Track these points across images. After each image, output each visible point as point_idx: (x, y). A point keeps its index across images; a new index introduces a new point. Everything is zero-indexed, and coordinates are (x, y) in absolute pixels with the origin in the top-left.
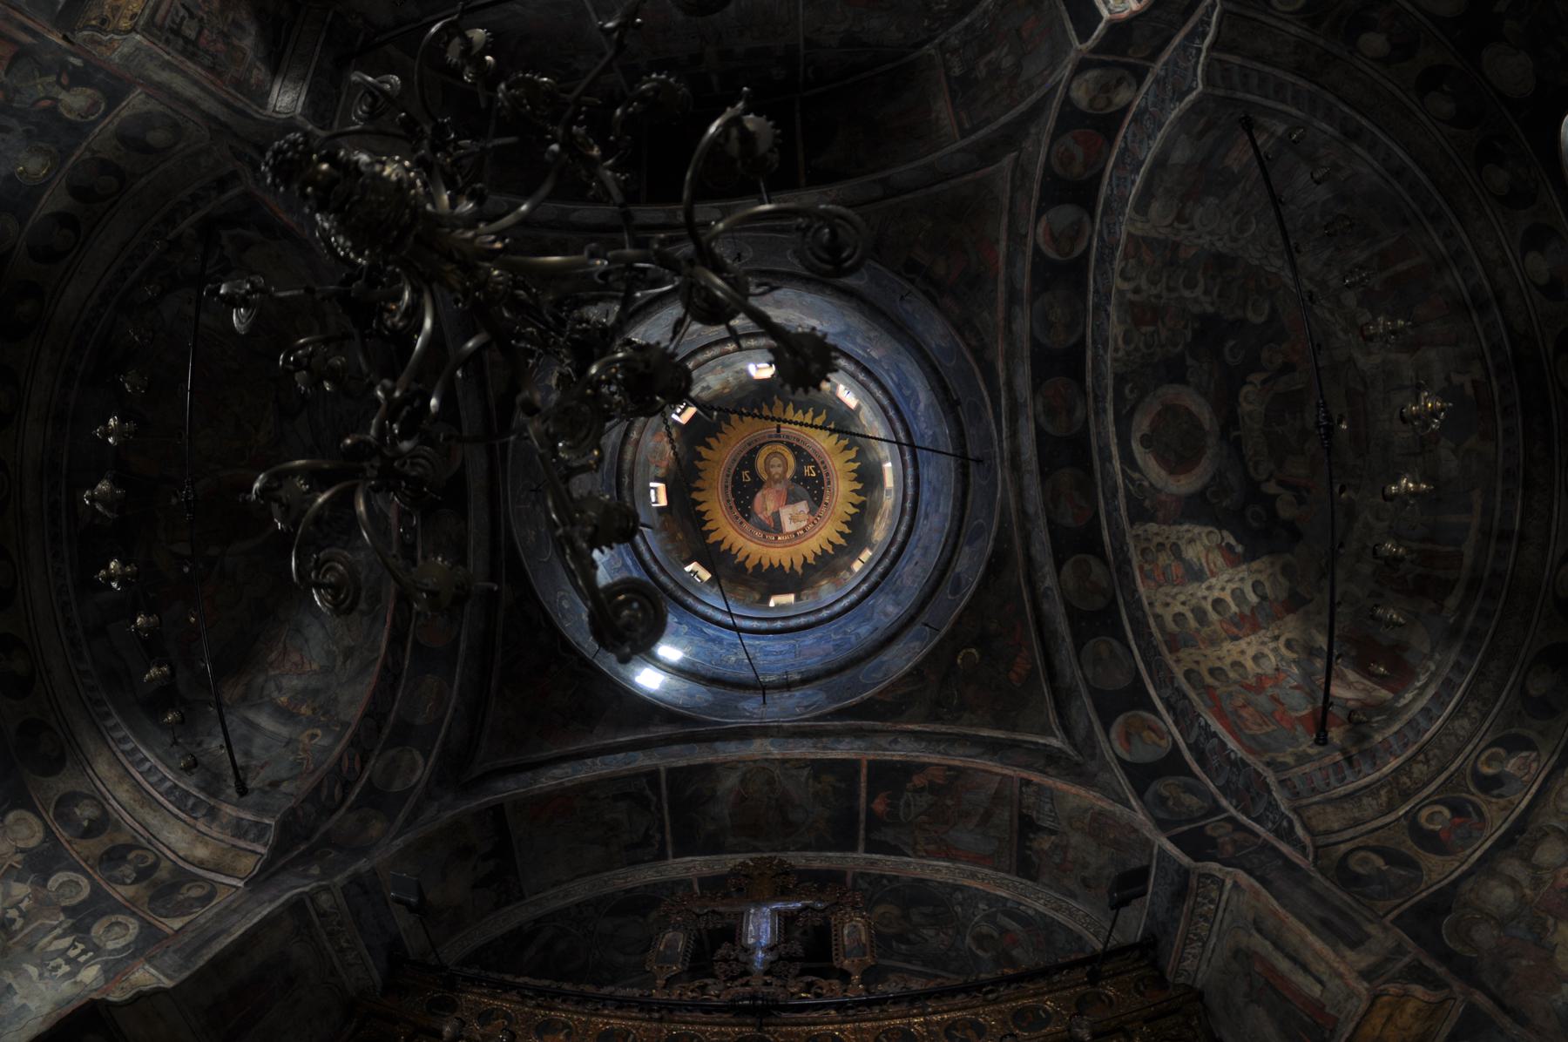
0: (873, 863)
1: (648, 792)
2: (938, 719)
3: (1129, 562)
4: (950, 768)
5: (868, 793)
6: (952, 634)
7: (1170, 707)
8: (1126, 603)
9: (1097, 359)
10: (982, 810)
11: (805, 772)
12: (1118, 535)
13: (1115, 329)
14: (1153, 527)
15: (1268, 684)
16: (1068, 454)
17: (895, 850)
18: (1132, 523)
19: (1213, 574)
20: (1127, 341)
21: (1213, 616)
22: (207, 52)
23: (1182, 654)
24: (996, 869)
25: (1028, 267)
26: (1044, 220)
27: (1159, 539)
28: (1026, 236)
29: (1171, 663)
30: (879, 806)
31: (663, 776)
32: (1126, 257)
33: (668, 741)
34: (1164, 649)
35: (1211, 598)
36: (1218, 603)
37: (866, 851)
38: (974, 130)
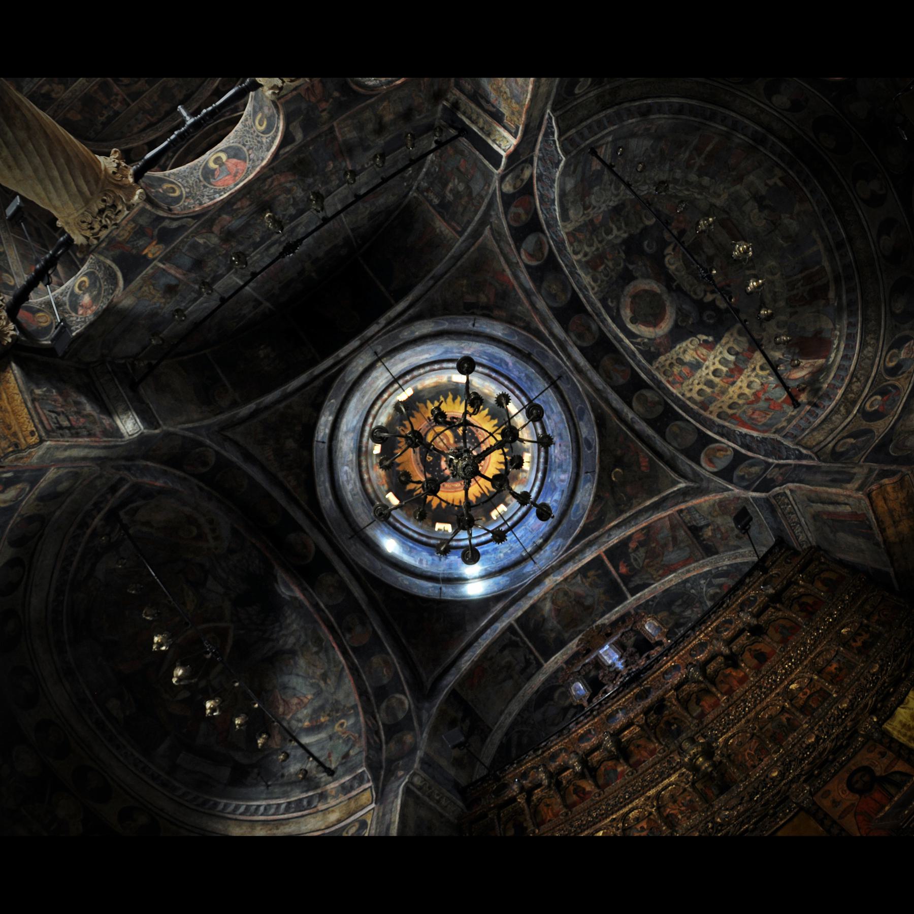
0: (639, 598)
1: (514, 638)
2: (622, 512)
3: (661, 382)
4: (643, 529)
5: (614, 567)
6: (602, 469)
7: (722, 435)
8: (672, 401)
11: (579, 578)
13: (586, 279)
14: (662, 359)
16: (601, 350)
18: (651, 364)
19: (705, 360)
20: (595, 280)
21: (717, 380)
23: (711, 409)
24: (697, 561)
25: (528, 277)
27: (668, 362)
28: (518, 263)
30: (623, 570)
32: (571, 244)
33: (505, 610)
34: (702, 412)
35: (710, 372)
36: (715, 373)
37: (632, 595)
38: (464, 230)
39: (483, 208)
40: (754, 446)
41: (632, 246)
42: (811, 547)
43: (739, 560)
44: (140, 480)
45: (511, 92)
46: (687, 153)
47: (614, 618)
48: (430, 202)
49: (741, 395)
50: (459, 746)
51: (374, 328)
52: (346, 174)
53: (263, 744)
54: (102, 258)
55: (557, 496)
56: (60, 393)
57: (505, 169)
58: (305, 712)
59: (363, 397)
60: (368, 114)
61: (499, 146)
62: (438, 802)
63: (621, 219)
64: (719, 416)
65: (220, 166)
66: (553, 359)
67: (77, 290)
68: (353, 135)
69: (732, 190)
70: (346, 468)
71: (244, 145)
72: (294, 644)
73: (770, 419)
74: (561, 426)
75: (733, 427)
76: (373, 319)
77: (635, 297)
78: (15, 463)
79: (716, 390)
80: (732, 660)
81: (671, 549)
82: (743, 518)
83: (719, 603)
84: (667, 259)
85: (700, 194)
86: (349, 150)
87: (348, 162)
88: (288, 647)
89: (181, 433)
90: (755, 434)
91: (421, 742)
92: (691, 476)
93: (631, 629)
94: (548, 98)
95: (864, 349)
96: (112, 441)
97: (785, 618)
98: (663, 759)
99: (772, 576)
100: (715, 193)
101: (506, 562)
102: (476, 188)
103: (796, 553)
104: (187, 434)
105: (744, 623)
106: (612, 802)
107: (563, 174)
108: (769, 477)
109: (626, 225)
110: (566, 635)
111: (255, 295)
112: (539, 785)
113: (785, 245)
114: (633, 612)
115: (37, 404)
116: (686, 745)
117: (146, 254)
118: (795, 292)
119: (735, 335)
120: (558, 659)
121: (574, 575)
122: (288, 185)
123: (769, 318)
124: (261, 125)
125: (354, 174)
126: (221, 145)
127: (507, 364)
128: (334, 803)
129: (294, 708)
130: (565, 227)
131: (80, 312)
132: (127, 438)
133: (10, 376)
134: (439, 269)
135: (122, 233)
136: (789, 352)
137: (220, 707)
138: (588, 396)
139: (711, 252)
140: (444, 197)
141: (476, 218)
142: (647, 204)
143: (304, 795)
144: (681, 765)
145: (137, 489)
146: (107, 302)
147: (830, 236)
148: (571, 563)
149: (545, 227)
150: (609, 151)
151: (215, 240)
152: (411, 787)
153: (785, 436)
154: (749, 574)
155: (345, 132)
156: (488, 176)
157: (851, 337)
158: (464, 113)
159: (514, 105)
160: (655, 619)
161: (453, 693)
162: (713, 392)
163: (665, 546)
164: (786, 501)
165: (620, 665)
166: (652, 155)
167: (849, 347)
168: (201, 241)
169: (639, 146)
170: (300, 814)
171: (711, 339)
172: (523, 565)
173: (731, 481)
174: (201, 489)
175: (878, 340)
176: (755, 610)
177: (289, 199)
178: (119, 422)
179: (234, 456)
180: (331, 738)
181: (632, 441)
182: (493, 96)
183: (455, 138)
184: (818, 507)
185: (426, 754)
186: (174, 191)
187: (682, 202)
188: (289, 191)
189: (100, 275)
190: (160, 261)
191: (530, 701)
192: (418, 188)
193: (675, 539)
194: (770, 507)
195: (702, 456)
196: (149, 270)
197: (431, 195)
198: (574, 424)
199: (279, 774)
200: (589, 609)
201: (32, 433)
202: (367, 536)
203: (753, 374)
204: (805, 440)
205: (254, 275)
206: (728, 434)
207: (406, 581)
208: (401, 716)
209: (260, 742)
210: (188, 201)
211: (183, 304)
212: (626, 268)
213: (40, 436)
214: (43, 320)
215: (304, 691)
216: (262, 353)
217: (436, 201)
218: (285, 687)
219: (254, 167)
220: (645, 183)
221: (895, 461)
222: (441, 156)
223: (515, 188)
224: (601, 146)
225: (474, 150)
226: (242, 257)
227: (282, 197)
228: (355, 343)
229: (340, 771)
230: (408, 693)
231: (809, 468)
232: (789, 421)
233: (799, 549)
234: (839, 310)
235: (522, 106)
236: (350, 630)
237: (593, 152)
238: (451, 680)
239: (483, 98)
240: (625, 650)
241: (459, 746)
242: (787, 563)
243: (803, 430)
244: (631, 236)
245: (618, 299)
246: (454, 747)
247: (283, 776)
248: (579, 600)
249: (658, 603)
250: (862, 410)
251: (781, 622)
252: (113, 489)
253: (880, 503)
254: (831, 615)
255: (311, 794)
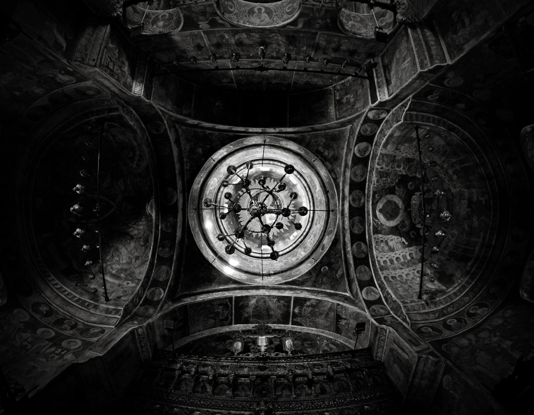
0: (294, 328)
1: (229, 304)
2: (315, 286)
4: (317, 300)
7: (380, 286)
9: (369, 186)
10: (326, 313)
11: (275, 300)
12: (370, 237)
13: (374, 179)
14: (380, 236)
15: (409, 282)
17: (301, 325)
20: (378, 182)
22: (116, 74)
23: (384, 272)
24: (329, 331)
25: (351, 158)
26: (357, 147)
29: (381, 274)
30: (296, 311)
31: (234, 299)
32: (379, 159)
33: (235, 289)
34: (379, 270)
39: (354, 116)
40: (389, 301)
41: (403, 180)
42: (380, 361)
43: (347, 344)
44: (124, 115)
45: (401, 77)
46: (455, 160)
47: (277, 328)
48: (335, 96)
49: (400, 276)
50: (169, 330)
51: (272, 130)
52: (307, 56)
53: (88, 265)
54: (180, 12)
55: (294, 259)
56: (119, 53)
57: (375, 107)
58: (117, 266)
59: (246, 155)
60: (336, 39)
61: (380, 95)
62: (142, 347)
63: (408, 165)
64: (385, 277)
65: (259, 13)
66: (336, 201)
67: (160, 17)
68: (323, 43)
69: (463, 189)
70: (216, 179)
71: (275, 12)
72: (135, 235)
73: (405, 295)
74: (318, 231)
75: (387, 286)
76: (274, 126)
77: (389, 202)
78: (77, 67)
79: (393, 266)
80: (310, 383)
81: (323, 317)
82: (361, 327)
83: (325, 354)
84: (414, 197)
85: (448, 181)
86: (317, 48)
87: (313, 53)
88: (131, 233)
89: (157, 109)
90: (393, 296)
91: (155, 316)
92: (354, 293)
93: (280, 338)
94: (415, 90)
95: (465, 296)
96: (125, 90)
97: (346, 382)
98: (248, 401)
99: (354, 361)
100: (455, 185)
101: (251, 270)
102: (358, 105)
103: (372, 359)
104: (159, 111)
105: (327, 371)
106: (213, 403)
107: (397, 127)
108: (385, 318)
109: (408, 170)
110: (252, 320)
111: (233, 77)
112: (189, 372)
113: (467, 229)
114: (287, 331)
115: (105, 50)
116: (262, 403)
117: (199, 24)
118: (455, 251)
119: (418, 250)
120: (241, 327)
121: (274, 297)
122: (281, 42)
123: (436, 252)
124: (288, 9)
125: (311, 59)
126: (266, 5)
127: (316, 189)
128: (98, 314)
129: (114, 261)
130: (382, 150)
131: (154, 27)
132: (133, 93)
133: (104, 29)
134: (317, 126)
135: (196, 8)
136: (434, 274)
137: (82, 235)
138: (338, 228)
139: (434, 208)
140: (342, 99)
141: (348, 118)
142: (424, 167)
143: (89, 301)
144: (254, 410)
145: (120, 117)
146: (168, 31)
147: (487, 240)
148: (277, 291)
149: (374, 144)
150: (424, 133)
151: (233, 41)
152: (135, 331)
153: (404, 307)
154: (346, 353)
155: (321, 39)
156: (366, 104)
157: (464, 287)
158: (376, 71)
159: (398, 83)
160: (293, 341)
161: (185, 306)
162: (390, 266)
163: (321, 314)
164: (384, 334)
165: (263, 349)
166: (441, 149)
167: (460, 291)
168: (227, 37)
169: (438, 141)
170: (81, 307)
171: (406, 243)
172: (257, 277)
173: (368, 308)
174: (147, 139)
175: (474, 297)
176: (336, 369)
177: (277, 49)
178: (134, 85)
179: (172, 137)
180: (119, 285)
181: (342, 260)
182: (393, 73)
183: (365, 78)
184: (395, 347)
185: (153, 323)
186: (231, 8)
187: (436, 176)
188: (279, 45)
189: (175, 18)
190: (204, 32)
191: (215, 335)
192: (335, 87)
193: (327, 314)
194: (376, 331)
195: (365, 288)
196: (196, 32)
197: (337, 94)
198: (324, 235)
199: (85, 284)
200: (269, 316)
201: (94, 60)
202: (202, 214)
203: (413, 272)
204: (411, 315)
205: (238, 68)
206: (383, 288)
207: (202, 245)
208: (156, 299)
209: (87, 263)
210: (234, 16)
211: (200, 57)
212: (394, 187)
213: (96, 64)
214: (136, 18)
215: (124, 257)
216: (217, 104)
217: (338, 98)
218: (117, 249)
219: (272, 24)
220: (429, 158)
221: (442, 352)
222: (354, 81)
223: (374, 117)
224: (422, 128)
225: (369, 89)
226: (238, 57)
227: (274, 46)
228: (259, 130)
229: (112, 302)
230: (166, 291)
231: (404, 327)
232: (412, 302)
233: (375, 358)
234: (468, 273)
235: (401, 86)
236: (163, 247)
237: (417, 128)
238: (188, 300)
239: (388, 70)
240: (270, 344)
241: (169, 330)
242: (365, 360)
243: (414, 310)
244: (406, 175)
245: (381, 197)
246: (166, 328)
247: (86, 286)
248: (268, 309)
249: (300, 336)
250: (445, 321)
251: (343, 383)
252: (111, 110)
253: (421, 365)
254: (366, 396)
255: (92, 302)
